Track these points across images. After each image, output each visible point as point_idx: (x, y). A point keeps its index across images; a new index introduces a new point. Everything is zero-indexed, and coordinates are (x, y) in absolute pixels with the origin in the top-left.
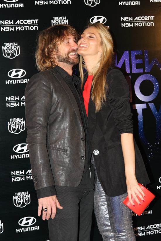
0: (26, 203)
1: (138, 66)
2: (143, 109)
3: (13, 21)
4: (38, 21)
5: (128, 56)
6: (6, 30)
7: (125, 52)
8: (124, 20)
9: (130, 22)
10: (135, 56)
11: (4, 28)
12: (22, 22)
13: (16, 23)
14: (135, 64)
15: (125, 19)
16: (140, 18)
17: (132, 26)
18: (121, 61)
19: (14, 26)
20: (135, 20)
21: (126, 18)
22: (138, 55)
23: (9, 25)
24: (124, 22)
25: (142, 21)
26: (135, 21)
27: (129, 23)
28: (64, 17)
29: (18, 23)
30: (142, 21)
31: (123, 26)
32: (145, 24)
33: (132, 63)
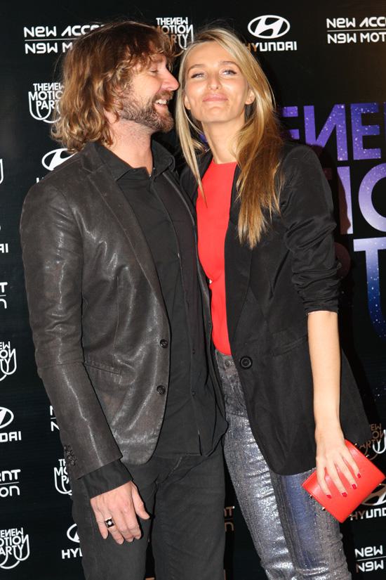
0: (18, 556)
1: (368, 143)
2: (380, 251)
3: (55, 28)
5: (344, 117)
6: (37, 50)
7: (335, 106)
8: (334, 26)
9: (349, 31)
10: (360, 118)
11: (34, 45)
13: (63, 34)
14: (361, 137)
15: (338, 23)
16: (374, 22)
17: (355, 41)
18: (327, 129)
19: (59, 40)
21: (340, 21)
22: (370, 114)
23: (46, 37)
24: (335, 31)
26: (361, 28)
27: (348, 32)
28: (184, 19)
29: (67, 33)
31: (331, 40)
33: (353, 135)
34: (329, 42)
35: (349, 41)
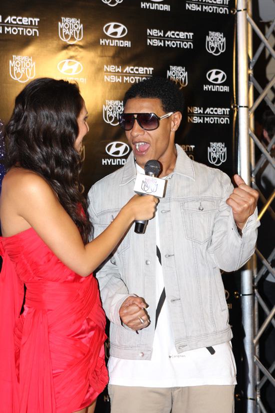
4: (38, 21)
9: (159, 38)
12: (15, 20)
13: (6, 21)
15: (154, 32)
17: (162, 45)
21: (155, 31)
24: (152, 37)
29: (8, 21)
31: (149, 43)
34: (148, 44)
35: (159, 45)
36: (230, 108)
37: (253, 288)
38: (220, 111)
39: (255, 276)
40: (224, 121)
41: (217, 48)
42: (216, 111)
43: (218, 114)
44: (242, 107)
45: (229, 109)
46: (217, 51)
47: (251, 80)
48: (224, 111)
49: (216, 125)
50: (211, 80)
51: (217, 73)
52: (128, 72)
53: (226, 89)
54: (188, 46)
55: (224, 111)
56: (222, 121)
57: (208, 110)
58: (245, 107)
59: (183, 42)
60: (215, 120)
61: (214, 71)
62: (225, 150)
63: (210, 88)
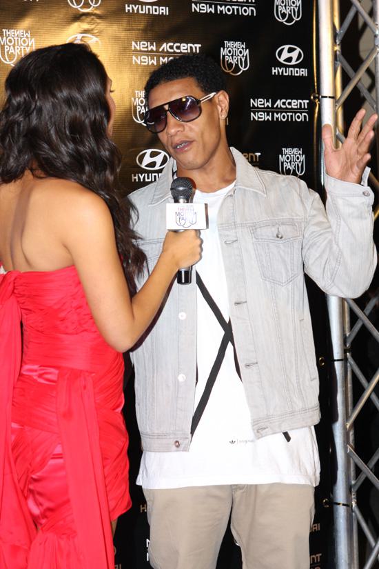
9: (267, 110)
15: (258, 103)
20: (275, 106)
21: (261, 101)
24: (256, 110)
25: (287, 110)
30: (287, 110)
32: (292, 116)
36: (309, 99)
37: (345, 351)
38: (295, 103)
39: (348, 334)
40: (301, 117)
41: (290, 15)
42: (290, 104)
43: (292, 108)
44: (326, 97)
45: (308, 101)
46: (290, 19)
47: (338, 59)
48: (300, 104)
49: (290, 124)
50: (281, 60)
51: (291, 50)
52: (165, 50)
53: (303, 72)
54: (249, 12)
55: (300, 104)
56: (299, 117)
57: (279, 103)
58: (330, 97)
59: (242, 7)
60: (288, 116)
61: (287, 47)
62: (303, 158)
63: (280, 71)
